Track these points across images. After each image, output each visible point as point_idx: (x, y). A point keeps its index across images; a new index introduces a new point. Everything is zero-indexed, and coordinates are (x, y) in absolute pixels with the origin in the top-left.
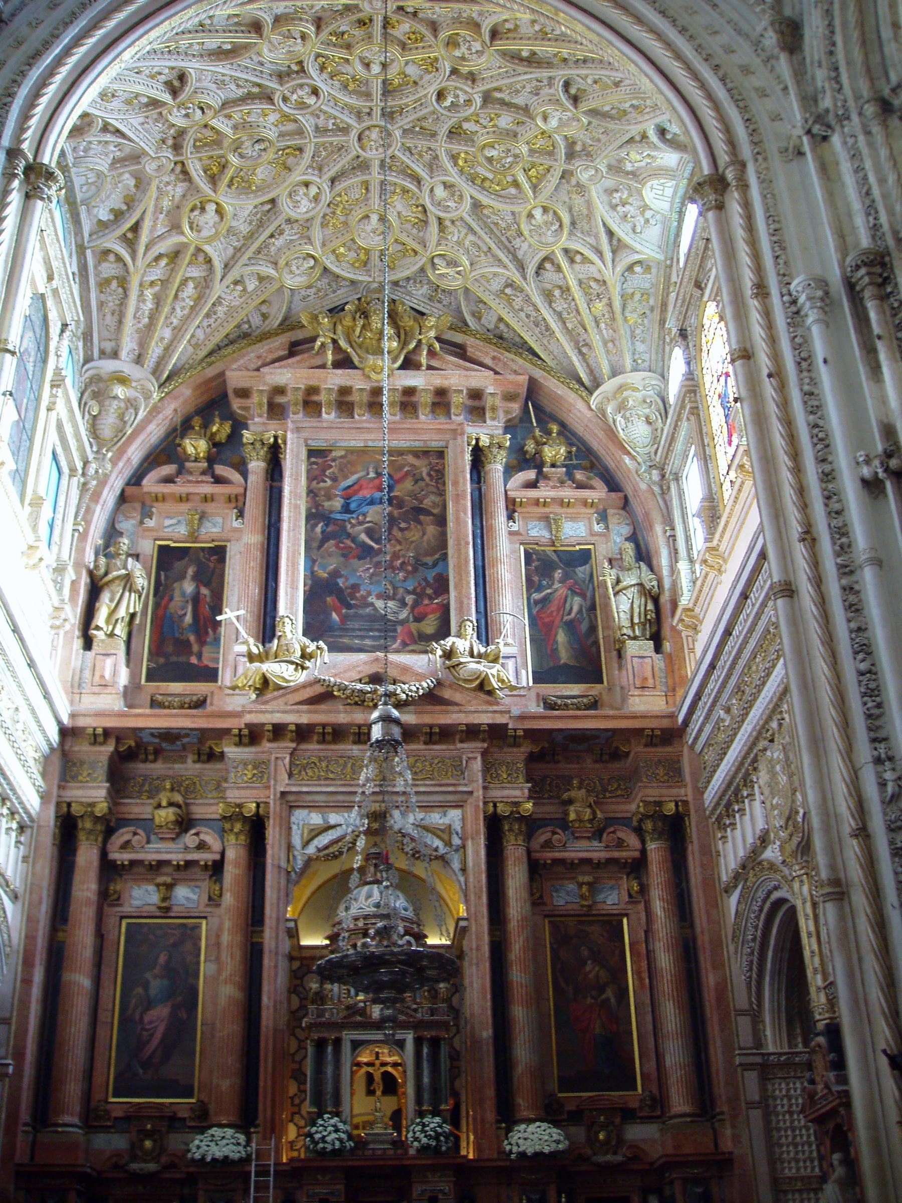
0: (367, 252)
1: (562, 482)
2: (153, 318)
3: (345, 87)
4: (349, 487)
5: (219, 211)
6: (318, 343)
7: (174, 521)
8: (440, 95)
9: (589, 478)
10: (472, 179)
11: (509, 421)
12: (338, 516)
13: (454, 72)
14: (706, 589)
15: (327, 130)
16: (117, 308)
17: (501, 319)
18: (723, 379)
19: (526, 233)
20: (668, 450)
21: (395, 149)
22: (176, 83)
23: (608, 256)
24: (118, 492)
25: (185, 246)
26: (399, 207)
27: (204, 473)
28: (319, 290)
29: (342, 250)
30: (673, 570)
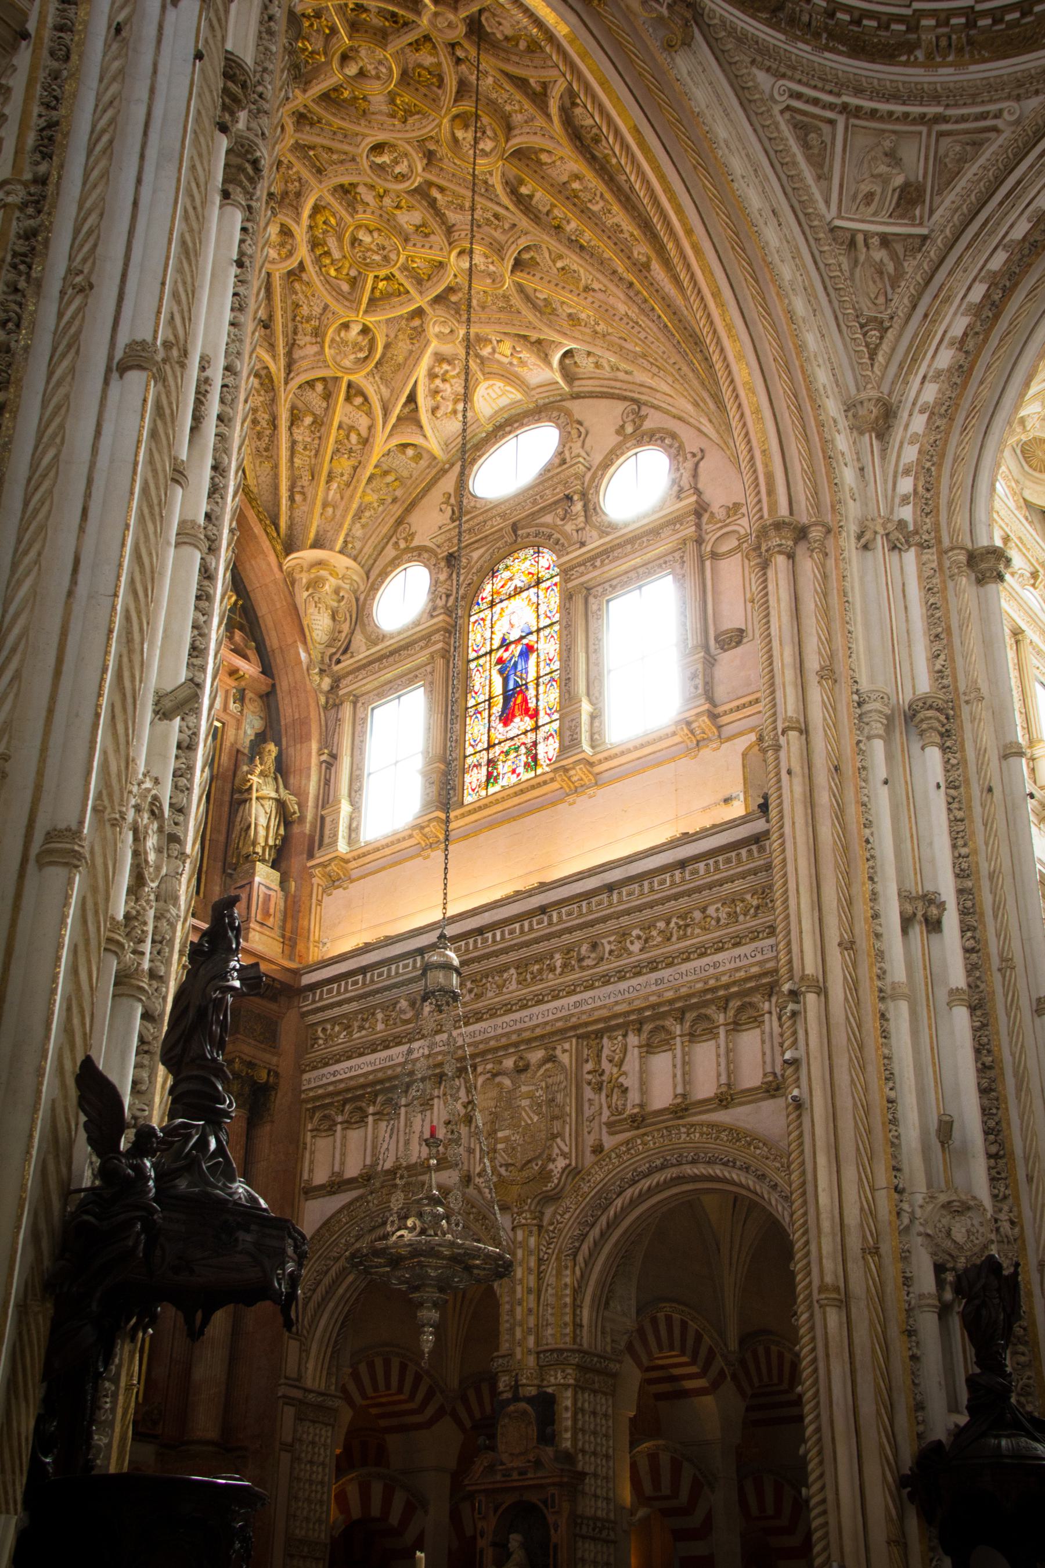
18: (516, 650)
20: (364, 667)
23: (393, 420)
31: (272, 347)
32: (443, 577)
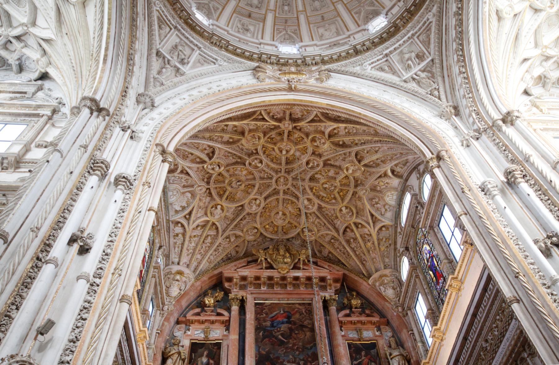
0: (278, 227)
1: (361, 314)
2: (194, 250)
3: (272, 161)
4: (273, 317)
5: (222, 209)
6: (259, 260)
7: (199, 332)
8: (308, 163)
9: (371, 313)
10: (318, 197)
11: (336, 291)
12: (269, 329)
13: (314, 153)
14: (435, 351)
15: (264, 178)
16: (180, 245)
17: (330, 252)
18: (430, 260)
19: (339, 217)
21: (289, 186)
22: (211, 155)
23: (372, 224)
24: (176, 319)
25: (208, 221)
26: (290, 209)
27: (212, 311)
28: (258, 242)
29: (267, 226)
30: (414, 349)
31: (329, 229)
32: (407, 255)
